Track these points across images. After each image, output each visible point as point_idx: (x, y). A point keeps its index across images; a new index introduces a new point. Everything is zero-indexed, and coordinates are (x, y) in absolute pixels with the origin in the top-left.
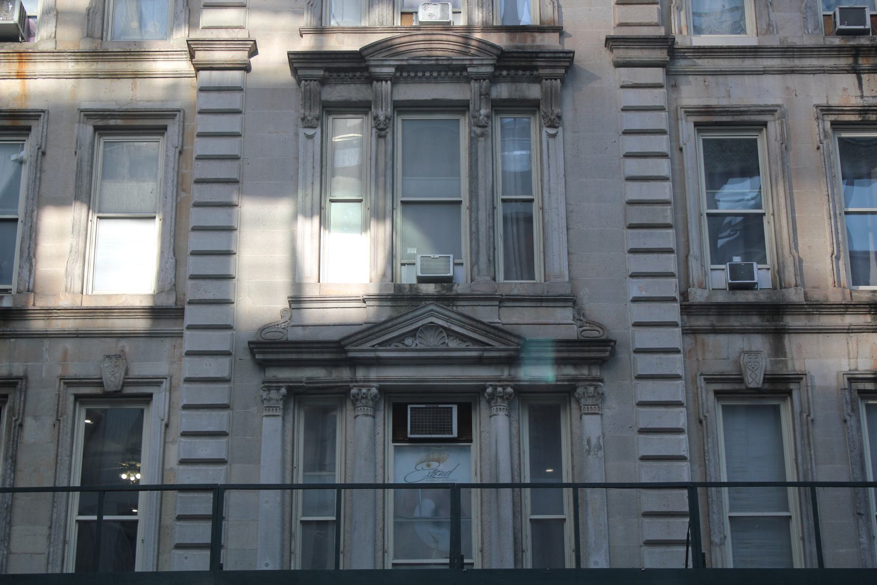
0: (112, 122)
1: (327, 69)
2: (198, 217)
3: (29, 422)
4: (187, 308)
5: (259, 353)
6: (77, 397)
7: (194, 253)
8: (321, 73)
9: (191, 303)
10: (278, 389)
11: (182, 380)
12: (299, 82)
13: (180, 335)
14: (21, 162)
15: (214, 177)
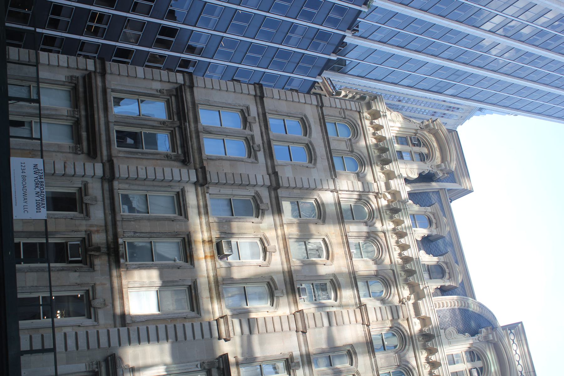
0: (193, 291)
1: (223, 369)
2: (162, 328)
3: (77, 274)
4: (126, 328)
5: (111, 358)
6: (88, 291)
7: (147, 328)
8: (222, 367)
9: (128, 329)
10: (97, 368)
11: (98, 330)
12: (217, 359)
13: (115, 327)
14: (175, 260)
15: (177, 331)
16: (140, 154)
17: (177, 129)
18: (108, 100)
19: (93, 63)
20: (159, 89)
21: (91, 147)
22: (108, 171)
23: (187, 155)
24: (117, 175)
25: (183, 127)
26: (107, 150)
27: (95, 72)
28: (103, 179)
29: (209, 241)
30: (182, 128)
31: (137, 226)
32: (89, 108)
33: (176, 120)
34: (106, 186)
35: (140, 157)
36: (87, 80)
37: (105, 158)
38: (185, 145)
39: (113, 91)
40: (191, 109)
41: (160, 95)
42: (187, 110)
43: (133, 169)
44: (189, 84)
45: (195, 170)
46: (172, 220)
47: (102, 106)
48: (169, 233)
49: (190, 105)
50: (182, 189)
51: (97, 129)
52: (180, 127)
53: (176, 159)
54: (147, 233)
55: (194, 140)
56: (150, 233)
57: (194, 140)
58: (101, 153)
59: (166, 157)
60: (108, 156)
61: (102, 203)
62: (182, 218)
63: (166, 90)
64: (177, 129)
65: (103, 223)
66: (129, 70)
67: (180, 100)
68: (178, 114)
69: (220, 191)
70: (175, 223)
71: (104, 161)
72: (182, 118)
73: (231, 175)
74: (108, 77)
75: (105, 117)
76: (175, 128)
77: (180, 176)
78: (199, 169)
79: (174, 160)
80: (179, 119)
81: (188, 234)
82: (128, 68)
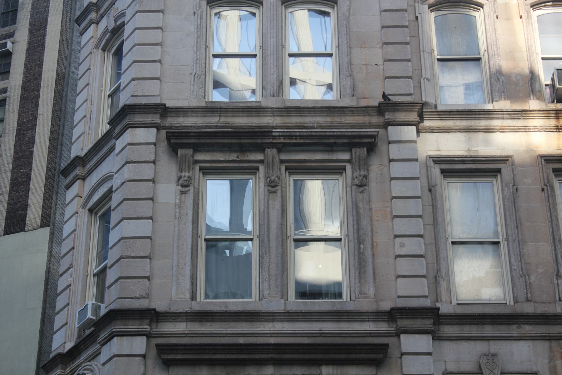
16: (362, 246)
17: (284, 157)
18: (224, 309)
19: (125, 338)
20: (179, 188)
21: (363, 356)
22: (418, 323)
23: (358, 141)
24: (427, 303)
25: (282, 141)
26: (363, 321)
27: (149, 336)
28: (437, 338)
29: (557, 118)
30: (284, 145)
31: (541, 270)
32: (257, 356)
33: (260, 157)
34: (448, 330)
35: (369, 247)
36: (179, 357)
37: (383, 327)
38: (332, 141)
39: (193, 297)
40: (223, 119)
41: (194, 187)
42: (227, 127)
43: (404, 266)
44: (158, 115)
45: (390, 128)
46: (515, 190)
47: (244, 324)
48: (549, 201)
49: (214, 120)
50: (435, 162)
51: (306, 341)
52: (282, 147)
53: (364, 164)
54: (555, 250)
55: (308, 120)
56: (554, 242)
57: (308, 120)
58: (370, 335)
59: (361, 189)
60: (376, 320)
61: (492, 343)
62: (506, 171)
63: (181, 170)
64: (284, 157)
65: (542, 347)
66: (133, 255)
67: (208, 141)
68: (242, 149)
69: (427, 79)
70: (520, 187)
71: (392, 329)
72: (259, 141)
73: (390, 48)
74: (160, 305)
75: (273, 321)
76: (282, 162)
77: (408, 163)
78: (387, 117)
79: (368, 171)
80: (261, 148)
81: (545, 160)
82: (128, 257)
